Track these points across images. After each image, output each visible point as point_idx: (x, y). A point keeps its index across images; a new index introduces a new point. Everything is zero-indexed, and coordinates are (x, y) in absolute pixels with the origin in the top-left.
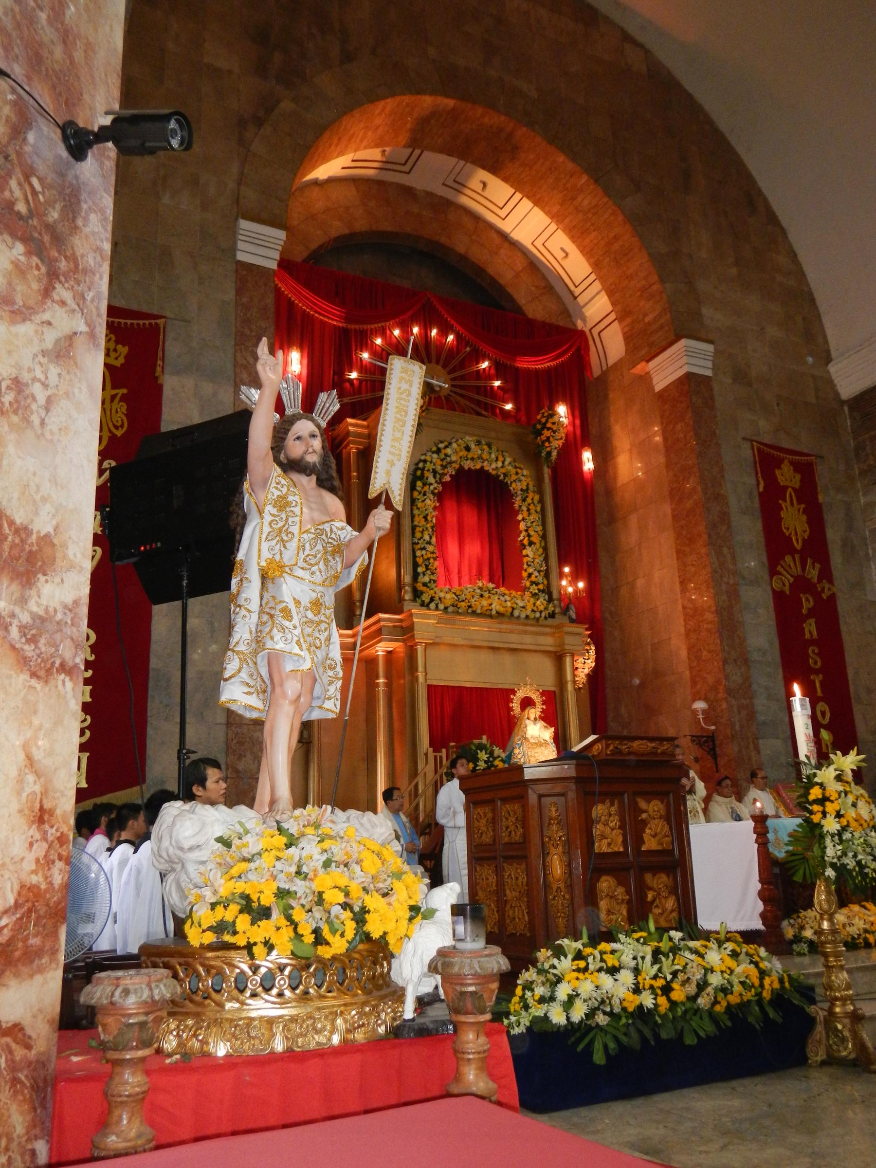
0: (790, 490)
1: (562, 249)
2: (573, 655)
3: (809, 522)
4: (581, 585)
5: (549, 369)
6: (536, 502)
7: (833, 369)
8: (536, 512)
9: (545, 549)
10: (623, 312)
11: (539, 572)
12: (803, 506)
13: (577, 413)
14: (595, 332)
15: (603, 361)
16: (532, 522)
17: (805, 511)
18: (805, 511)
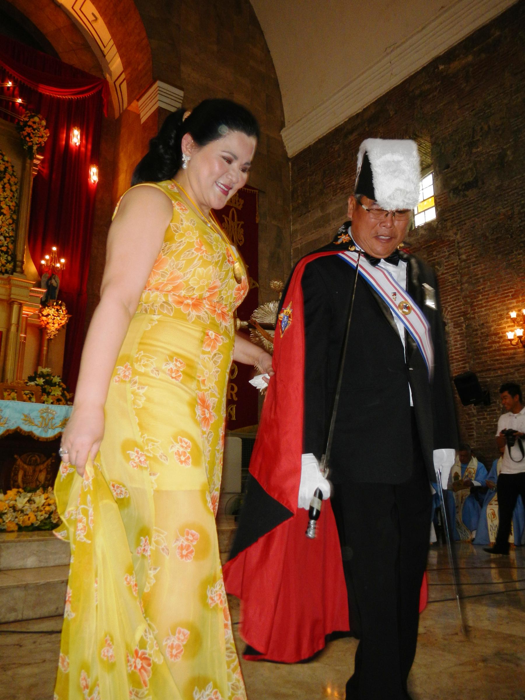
0: (233, 209)
1: (93, 14)
2: (21, 305)
3: (245, 235)
4: (63, 261)
5: (70, 101)
6: (12, 183)
7: (284, 133)
8: (11, 190)
9: (16, 222)
10: (127, 64)
11: (5, 237)
12: (242, 223)
13: (90, 140)
14: (117, 84)
15: (121, 104)
16: (6, 198)
17: (242, 226)
18: (242, 226)
